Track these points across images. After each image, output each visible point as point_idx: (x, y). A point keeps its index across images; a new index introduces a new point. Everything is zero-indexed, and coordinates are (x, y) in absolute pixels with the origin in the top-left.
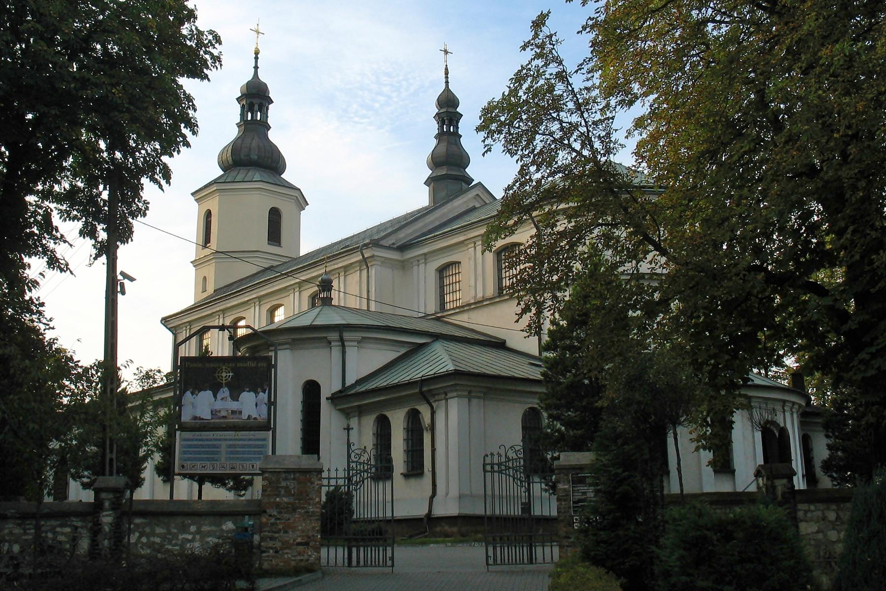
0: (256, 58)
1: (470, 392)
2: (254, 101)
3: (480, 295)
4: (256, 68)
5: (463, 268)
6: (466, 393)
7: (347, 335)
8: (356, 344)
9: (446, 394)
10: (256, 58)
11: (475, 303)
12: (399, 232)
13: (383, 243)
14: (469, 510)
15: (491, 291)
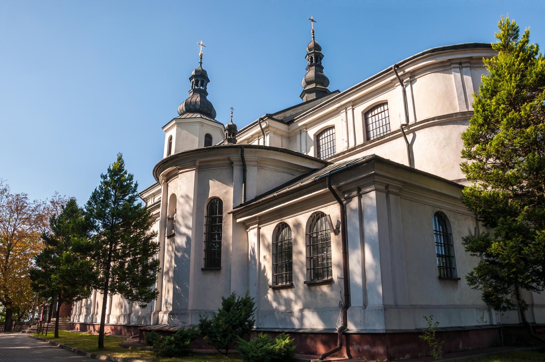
0: (201, 58)
1: (387, 187)
2: (199, 79)
3: (352, 145)
4: (201, 63)
5: (337, 130)
6: (383, 188)
7: (249, 156)
8: (256, 163)
9: (359, 189)
10: (201, 58)
11: (349, 151)
12: (286, 112)
13: (274, 117)
14: (395, 327)
15: (360, 140)
